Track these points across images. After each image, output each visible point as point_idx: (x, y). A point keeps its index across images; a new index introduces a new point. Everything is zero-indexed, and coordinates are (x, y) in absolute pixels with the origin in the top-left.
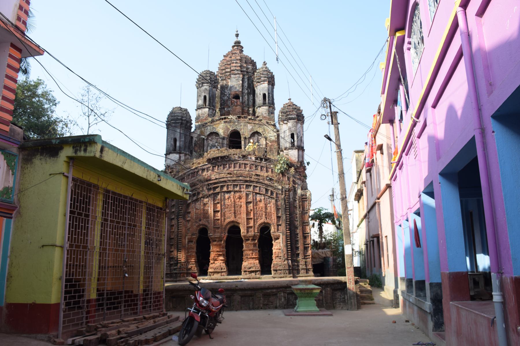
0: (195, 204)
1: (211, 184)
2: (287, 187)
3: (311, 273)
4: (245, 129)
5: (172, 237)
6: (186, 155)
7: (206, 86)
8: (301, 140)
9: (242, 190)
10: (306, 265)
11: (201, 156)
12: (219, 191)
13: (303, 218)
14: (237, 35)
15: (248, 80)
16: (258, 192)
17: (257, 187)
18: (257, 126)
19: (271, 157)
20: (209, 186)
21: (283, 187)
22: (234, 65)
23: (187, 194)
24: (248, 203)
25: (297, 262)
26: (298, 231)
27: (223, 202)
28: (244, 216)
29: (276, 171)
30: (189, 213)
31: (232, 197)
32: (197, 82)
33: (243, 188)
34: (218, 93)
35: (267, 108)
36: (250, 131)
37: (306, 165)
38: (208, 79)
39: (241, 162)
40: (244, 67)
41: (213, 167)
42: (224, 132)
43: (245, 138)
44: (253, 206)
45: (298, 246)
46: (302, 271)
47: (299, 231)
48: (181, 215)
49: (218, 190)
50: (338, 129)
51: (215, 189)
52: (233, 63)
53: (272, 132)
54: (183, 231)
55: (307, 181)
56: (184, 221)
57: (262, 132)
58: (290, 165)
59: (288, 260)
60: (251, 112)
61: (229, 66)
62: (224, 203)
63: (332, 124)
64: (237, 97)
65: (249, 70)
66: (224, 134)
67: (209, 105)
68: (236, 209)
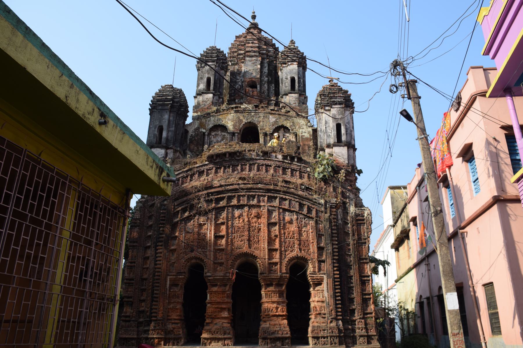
0: (186, 224)
1: (212, 193)
2: (334, 200)
4: (266, 122)
5: (145, 276)
6: (175, 151)
10: (366, 329)
11: (198, 153)
12: (224, 205)
14: (254, 17)
15: (269, 65)
16: (287, 207)
17: (285, 199)
18: (283, 118)
19: (305, 158)
20: (208, 196)
21: (326, 202)
23: (168, 181)
24: (270, 225)
26: (352, 272)
27: (230, 223)
28: (264, 245)
29: (316, 175)
31: (245, 214)
33: (263, 201)
34: (228, 77)
35: (296, 95)
36: (273, 125)
39: (261, 162)
40: (264, 49)
41: (217, 168)
42: (234, 126)
43: (265, 135)
44: (280, 229)
45: (353, 296)
47: (353, 272)
48: (161, 241)
49: (222, 204)
50: (419, 105)
51: (220, 200)
52: (249, 43)
53: (305, 127)
55: (360, 196)
56: (165, 251)
57: (291, 126)
58: (336, 169)
59: (337, 320)
61: (243, 48)
62: (232, 224)
63: (409, 98)
65: (271, 54)
66: (234, 128)
67: (214, 89)
68: (252, 233)
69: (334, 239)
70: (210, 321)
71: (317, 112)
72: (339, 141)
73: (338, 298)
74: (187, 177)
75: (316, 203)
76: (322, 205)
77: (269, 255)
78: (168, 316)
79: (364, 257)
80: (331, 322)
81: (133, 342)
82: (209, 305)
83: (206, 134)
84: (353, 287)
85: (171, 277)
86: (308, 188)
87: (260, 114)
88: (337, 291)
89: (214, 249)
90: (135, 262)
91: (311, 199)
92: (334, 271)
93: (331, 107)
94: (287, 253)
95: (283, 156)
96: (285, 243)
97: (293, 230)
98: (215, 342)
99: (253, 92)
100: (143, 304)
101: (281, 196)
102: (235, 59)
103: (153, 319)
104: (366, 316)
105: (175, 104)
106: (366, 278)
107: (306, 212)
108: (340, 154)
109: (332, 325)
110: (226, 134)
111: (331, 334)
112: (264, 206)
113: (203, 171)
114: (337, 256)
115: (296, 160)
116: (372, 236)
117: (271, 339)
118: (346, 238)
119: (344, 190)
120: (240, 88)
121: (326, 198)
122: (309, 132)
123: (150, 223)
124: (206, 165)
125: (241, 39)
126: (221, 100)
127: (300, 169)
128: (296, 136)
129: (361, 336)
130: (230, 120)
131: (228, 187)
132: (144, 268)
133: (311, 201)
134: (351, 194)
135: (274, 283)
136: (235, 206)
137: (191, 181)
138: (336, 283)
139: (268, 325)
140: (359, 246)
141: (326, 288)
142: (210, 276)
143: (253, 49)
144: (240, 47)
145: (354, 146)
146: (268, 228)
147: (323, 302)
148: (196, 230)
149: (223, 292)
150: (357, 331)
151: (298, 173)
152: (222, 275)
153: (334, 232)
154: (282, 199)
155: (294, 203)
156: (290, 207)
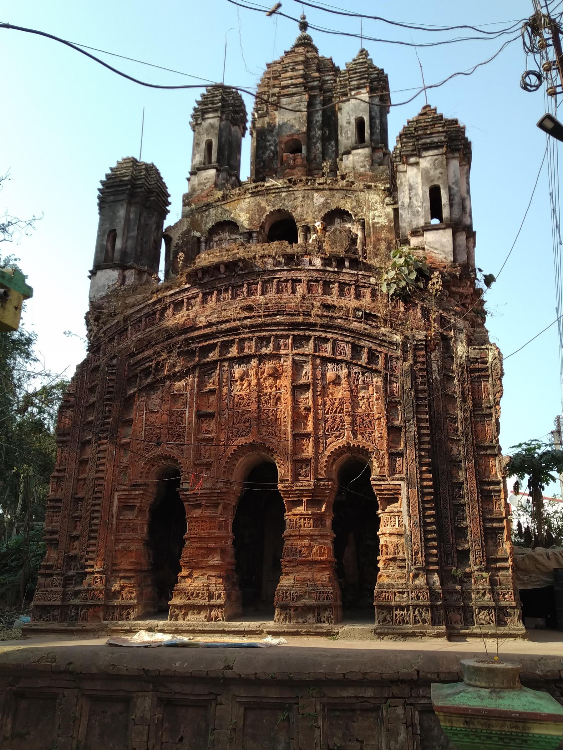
1: (193, 339)
2: (421, 335)
3: (516, 624)
4: (308, 206)
7: (212, 120)
8: (462, 204)
9: (283, 352)
10: (492, 591)
13: (475, 433)
17: (326, 340)
18: (338, 195)
22: (289, 74)
24: (298, 389)
25: (461, 583)
27: (225, 390)
29: (384, 289)
30: (130, 422)
31: (252, 372)
32: (193, 116)
33: (286, 345)
35: (366, 151)
36: (320, 211)
37: (480, 284)
39: (284, 275)
40: (314, 79)
41: (205, 295)
42: (251, 220)
45: (464, 523)
46: (483, 615)
47: (465, 475)
49: (213, 355)
52: (287, 71)
53: (379, 206)
54: (108, 476)
56: (112, 447)
61: (277, 82)
62: (230, 391)
64: (295, 148)
66: (251, 223)
67: (218, 161)
69: (420, 409)
73: (429, 528)
74: (155, 313)
75: (385, 341)
77: (294, 445)
78: (114, 565)
79: (487, 443)
80: (416, 576)
81: (56, 613)
83: (202, 239)
84: (465, 505)
85: (121, 493)
86: (370, 314)
87: (296, 193)
88: (428, 513)
89: (196, 439)
90: (64, 470)
91: (374, 335)
92: (422, 472)
93: (420, 157)
94: (329, 441)
95: (322, 258)
98: (193, 613)
99: (294, 160)
100: (76, 543)
101: (318, 334)
104: (493, 566)
105: (139, 190)
106: (491, 487)
107: (366, 361)
109: (417, 582)
110: (237, 236)
111: (416, 602)
112: (286, 355)
113: (182, 301)
114: (428, 443)
115: (347, 264)
116: (503, 402)
117: (296, 609)
118: (450, 407)
119: (445, 314)
120: (273, 157)
121: (406, 332)
122: (387, 216)
123: (92, 400)
124: (187, 290)
125: (275, 68)
127: (357, 281)
128: (363, 225)
129: (482, 608)
130: (243, 212)
131: (223, 326)
132: (79, 480)
133: (376, 338)
135: (304, 499)
136: (234, 358)
138: (427, 498)
139: (292, 581)
140: (476, 423)
142: (187, 490)
143: (294, 81)
145: (470, 227)
147: (400, 535)
151: (352, 289)
152: (209, 486)
155: (342, 345)
156: (334, 353)
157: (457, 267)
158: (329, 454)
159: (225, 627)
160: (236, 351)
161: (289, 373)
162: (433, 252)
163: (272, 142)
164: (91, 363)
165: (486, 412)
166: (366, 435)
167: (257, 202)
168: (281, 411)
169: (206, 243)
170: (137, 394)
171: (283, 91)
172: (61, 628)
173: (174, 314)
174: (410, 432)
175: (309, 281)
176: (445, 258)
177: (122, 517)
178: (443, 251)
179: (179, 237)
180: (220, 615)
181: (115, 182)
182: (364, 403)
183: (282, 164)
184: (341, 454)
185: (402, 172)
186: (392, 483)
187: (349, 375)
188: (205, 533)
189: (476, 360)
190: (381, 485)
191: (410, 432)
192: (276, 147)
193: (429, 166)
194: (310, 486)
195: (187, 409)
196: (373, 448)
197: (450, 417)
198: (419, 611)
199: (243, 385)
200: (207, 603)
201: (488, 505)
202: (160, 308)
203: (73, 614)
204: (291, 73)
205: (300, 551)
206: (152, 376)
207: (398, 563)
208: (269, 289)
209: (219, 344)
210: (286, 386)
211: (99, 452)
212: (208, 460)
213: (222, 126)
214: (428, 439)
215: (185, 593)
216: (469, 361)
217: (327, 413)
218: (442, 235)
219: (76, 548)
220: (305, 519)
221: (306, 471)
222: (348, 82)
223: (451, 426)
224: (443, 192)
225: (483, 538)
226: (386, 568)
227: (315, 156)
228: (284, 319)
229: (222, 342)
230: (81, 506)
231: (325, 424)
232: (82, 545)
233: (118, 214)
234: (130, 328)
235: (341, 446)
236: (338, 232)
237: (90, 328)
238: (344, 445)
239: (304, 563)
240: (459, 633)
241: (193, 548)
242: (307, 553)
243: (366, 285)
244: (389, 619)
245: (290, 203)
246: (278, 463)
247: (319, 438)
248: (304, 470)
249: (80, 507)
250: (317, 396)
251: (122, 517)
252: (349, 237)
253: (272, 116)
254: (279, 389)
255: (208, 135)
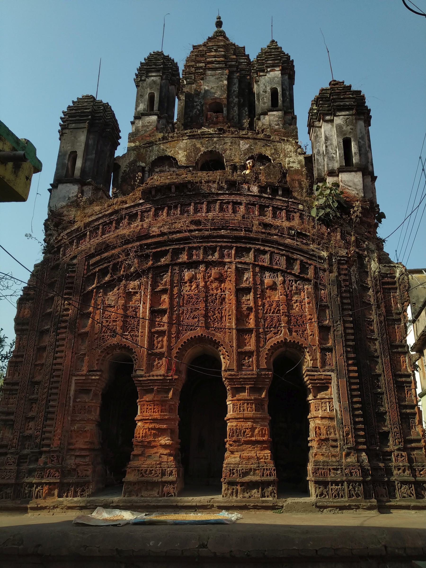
0: (105, 293)
1: (148, 246)
2: (343, 252)
5: (38, 378)
14: (219, 24)
15: (240, 82)
17: (264, 252)
24: (240, 292)
27: (176, 290)
31: (200, 276)
33: (229, 256)
35: (280, 113)
36: (245, 154)
38: (157, 65)
39: (226, 198)
41: (157, 210)
42: (188, 157)
53: (293, 154)
57: (272, 155)
58: (344, 205)
60: (246, 125)
62: (180, 291)
68: (211, 306)
69: (346, 313)
70: (140, 452)
71: (311, 125)
72: (348, 165)
73: (357, 413)
74: (111, 223)
75: (314, 256)
76: (325, 260)
77: (238, 339)
78: (69, 444)
79: (397, 343)
80: (348, 455)
81: (9, 491)
82: (139, 424)
83: (147, 169)
84: (383, 394)
87: (226, 139)
88: (355, 400)
90: (22, 356)
92: (349, 365)
93: (335, 115)
95: (259, 187)
96: (265, 320)
97: (277, 300)
98: (147, 490)
100: (31, 424)
101: (258, 247)
102: (192, 75)
103: (44, 449)
104: (409, 446)
105: (97, 121)
106: (404, 379)
107: (299, 271)
108: (351, 181)
109: (349, 460)
112: (230, 263)
113: (136, 214)
114: (353, 340)
115: (280, 193)
117: (242, 484)
120: (199, 114)
124: (141, 204)
126: (170, 125)
127: (287, 207)
129: (403, 483)
130: (181, 151)
134: (371, 243)
135: (247, 387)
137: (116, 228)
139: (238, 459)
140: (389, 325)
141: (336, 395)
142: (142, 376)
144: (198, 59)
145: (373, 173)
146: (237, 296)
147: (331, 419)
148: (121, 302)
149: (163, 401)
150: (395, 472)
151: (283, 213)
153: (345, 301)
154: (259, 252)
155: (278, 257)
156: (271, 263)
157: (366, 202)
158: (269, 347)
159: (178, 502)
160: (186, 257)
161: (233, 277)
162: (347, 188)
163: (198, 103)
164: (51, 262)
165: (397, 317)
166: (300, 332)
167: (193, 143)
168: (225, 310)
169: (149, 172)
170: (95, 290)
171: (209, 65)
172: (14, 505)
173: (129, 224)
174: (338, 331)
175: (248, 204)
176: (357, 194)
177: (78, 400)
178: (356, 188)
179: (127, 165)
180: (172, 491)
181: (76, 113)
182: (297, 306)
183: (206, 120)
184: (278, 348)
185: (318, 127)
186: (324, 373)
187: (284, 282)
188: (157, 415)
189: (385, 275)
190: (314, 375)
191: (338, 331)
192: (202, 106)
193: (342, 123)
194: (253, 375)
195: (141, 305)
196: (306, 344)
197: (367, 320)
198: (352, 486)
199: (192, 286)
200: (160, 480)
201: (401, 394)
202: (116, 218)
203: (27, 492)
204: (215, 53)
205: (244, 432)
206: (109, 276)
207: (331, 443)
208: (212, 209)
209: (170, 250)
210: (230, 289)
211: (57, 340)
212: (160, 350)
213: (162, 84)
214: (353, 337)
215: (139, 470)
216: (381, 276)
217: (266, 313)
218: (354, 176)
219: (31, 429)
220: (248, 404)
221: (249, 362)
222: (264, 61)
223: (368, 327)
224: (353, 144)
225: (400, 422)
226: (320, 447)
227: (233, 117)
228: (228, 233)
229: (173, 249)
230: (38, 390)
231: (265, 322)
232: (38, 426)
233: (79, 139)
234: (88, 233)
235: (280, 341)
236: (272, 167)
237: (49, 232)
238: (282, 341)
239: (247, 443)
240: (386, 506)
241: (146, 429)
242: (250, 434)
243: (295, 210)
244: (325, 493)
245: (221, 146)
246: (223, 354)
247: (260, 334)
248: (247, 361)
249: (36, 389)
250: (258, 298)
251: (78, 400)
252: (281, 171)
253: (198, 83)
254: (224, 291)
255: (151, 89)
